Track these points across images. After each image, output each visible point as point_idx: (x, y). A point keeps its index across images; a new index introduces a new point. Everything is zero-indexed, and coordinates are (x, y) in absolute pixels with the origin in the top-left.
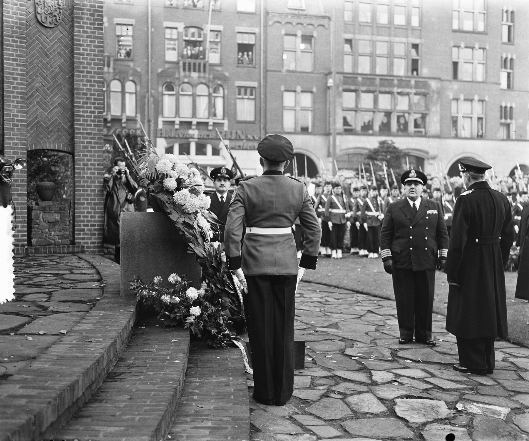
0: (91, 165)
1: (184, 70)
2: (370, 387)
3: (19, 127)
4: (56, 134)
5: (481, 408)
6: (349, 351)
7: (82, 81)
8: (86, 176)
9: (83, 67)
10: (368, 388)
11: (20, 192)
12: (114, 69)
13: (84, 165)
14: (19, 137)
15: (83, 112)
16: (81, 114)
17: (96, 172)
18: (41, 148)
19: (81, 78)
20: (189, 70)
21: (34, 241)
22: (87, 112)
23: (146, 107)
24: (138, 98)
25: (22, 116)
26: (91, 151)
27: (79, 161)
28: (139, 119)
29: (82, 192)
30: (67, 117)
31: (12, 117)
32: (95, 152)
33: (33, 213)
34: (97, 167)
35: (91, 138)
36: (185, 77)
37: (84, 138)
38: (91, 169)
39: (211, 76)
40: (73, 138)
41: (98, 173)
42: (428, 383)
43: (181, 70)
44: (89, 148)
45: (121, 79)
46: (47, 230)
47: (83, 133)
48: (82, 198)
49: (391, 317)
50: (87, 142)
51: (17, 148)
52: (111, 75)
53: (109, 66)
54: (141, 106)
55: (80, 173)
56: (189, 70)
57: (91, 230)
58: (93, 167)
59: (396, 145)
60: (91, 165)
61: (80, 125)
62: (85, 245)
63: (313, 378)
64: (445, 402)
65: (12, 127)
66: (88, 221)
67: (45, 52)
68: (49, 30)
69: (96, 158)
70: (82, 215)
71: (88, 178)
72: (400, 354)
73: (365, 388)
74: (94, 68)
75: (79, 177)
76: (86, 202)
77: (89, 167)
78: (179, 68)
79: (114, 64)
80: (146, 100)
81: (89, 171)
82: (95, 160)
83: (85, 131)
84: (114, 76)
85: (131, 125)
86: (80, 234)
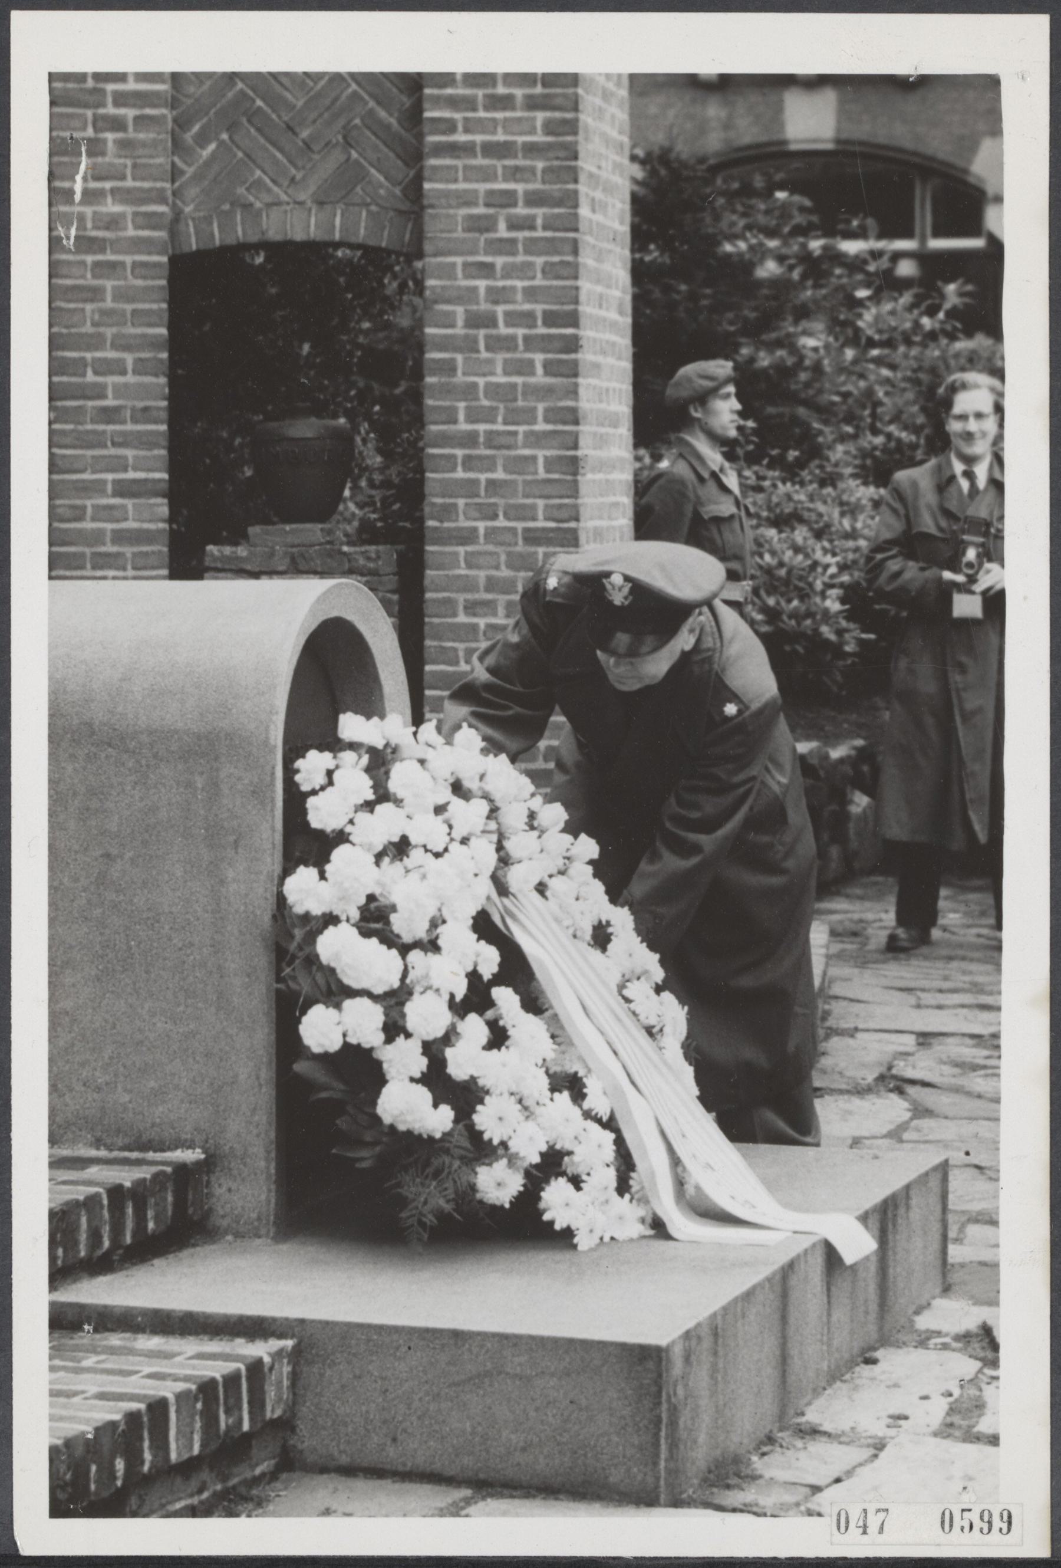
0: (512, 319)
3: (131, 134)
4: (337, 157)
8: (481, 381)
11: (131, 475)
13: (475, 321)
14: (129, 183)
17: (539, 358)
18: (254, 238)
26: (507, 247)
27: (448, 301)
29: (460, 474)
32: (532, 247)
34: (542, 330)
35: (514, 174)
37: (471, 174)
38: (508, 344)
41: (547, 366)
44: (502, 225)
47: (468, 149)
48: (461, 502)
50: (491, 193)
55: (450, 368)
58: (520, 332)
60: (512, 319)
61: (453, 103)
69: (539, 281)
70: (461, 598)
71: (493, 391)
75: (448, 391)
76: (481, 526)
77: (503, 330)
81: (500, 357)
82: (531, 294)
83: (479, 138)
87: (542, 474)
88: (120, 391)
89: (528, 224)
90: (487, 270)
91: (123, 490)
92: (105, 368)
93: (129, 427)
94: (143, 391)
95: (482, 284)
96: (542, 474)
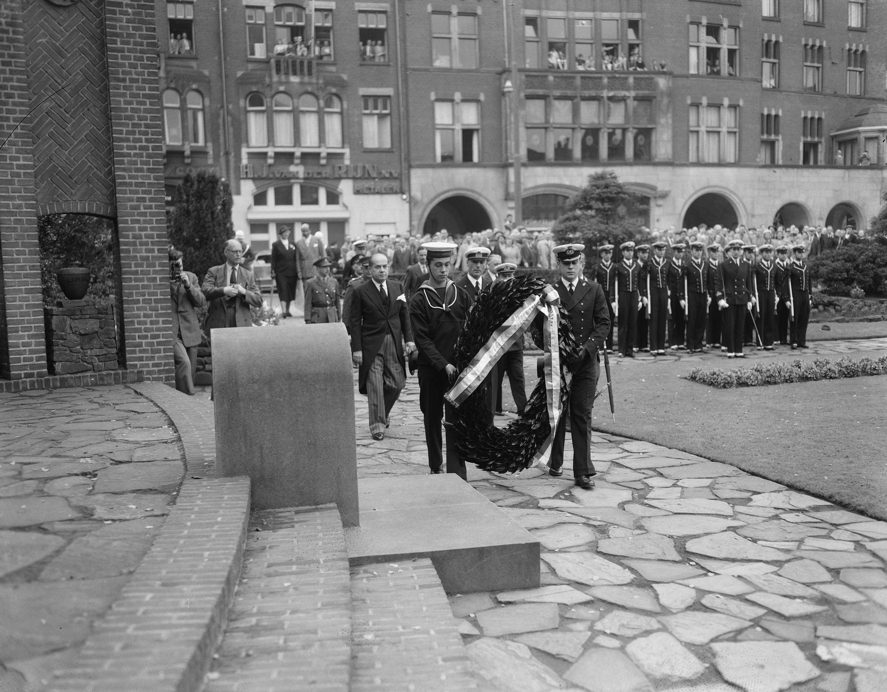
0: (147, 236)
1: (278, 71)
2: (660, 618)
3: (22, 178)
5: (858, 653)
6: (605, 546)
7: (124, 95)
8: (138, 255)
9: (124, 73)
10: (659, 622)
11: (30, 287)
12: (167, 72)
13: (134, 237)
15: (129, 148)
16: (125, 151)
17: (156, 248)
19: (122, 91)
20: (287, 74)
21: (58, 366)
22: (135, 148)
23: (221, 132)
24: (208, 116)
25: (25, 159)
26: (144, 214)
28: (210, 150)
29: (133, 283)
30: (101, 158)
31: (8, 162)
32: (152, 214)
33: (55, 320)
35: (144, 192)
36: (280, 83)
37: (131, 192)
38: (146, 244)
39: (321, 81)
40: (113, 193)
41: (158, 250)
42: (754, 603)
43: (274, 71)
44: (142, 208)
45: (179, 89)
46: (79, 347)
47: (130, 184)
49: (651, 473)
50: (138, 198)
51: (21, 214)
54: (212, 132)
56: (287, 74)
57: (152, 344)
59: (620, 181)
61: (124, 170)
62: (145, 369)
63: (563, 606)
64: (797, 643)
65: (9, 177)
66: (146, 330)
67: (58, 48)
68: (61, 11)
71: (142, 258)
72: (691, 546)
73: (653, 623)
74: (142, 74)
75: (128, 258)
76: (141, 298)
77: (144, 240)
78: (270, 70)
79: (166, 65)
80: (221, 121)
82: (152, 229)
83: (134, 181)
84: (167, 83)
85: (199, 161)
86: (134, 352)
87: (158, 282)
88: (25, 260)
89: (150, 207)
90: (138, 221)
91: (28, 291)
92: (19, 253)
93: (29, 272)
94: (32, 261)
95: (137, 226)
96: (158, 282)
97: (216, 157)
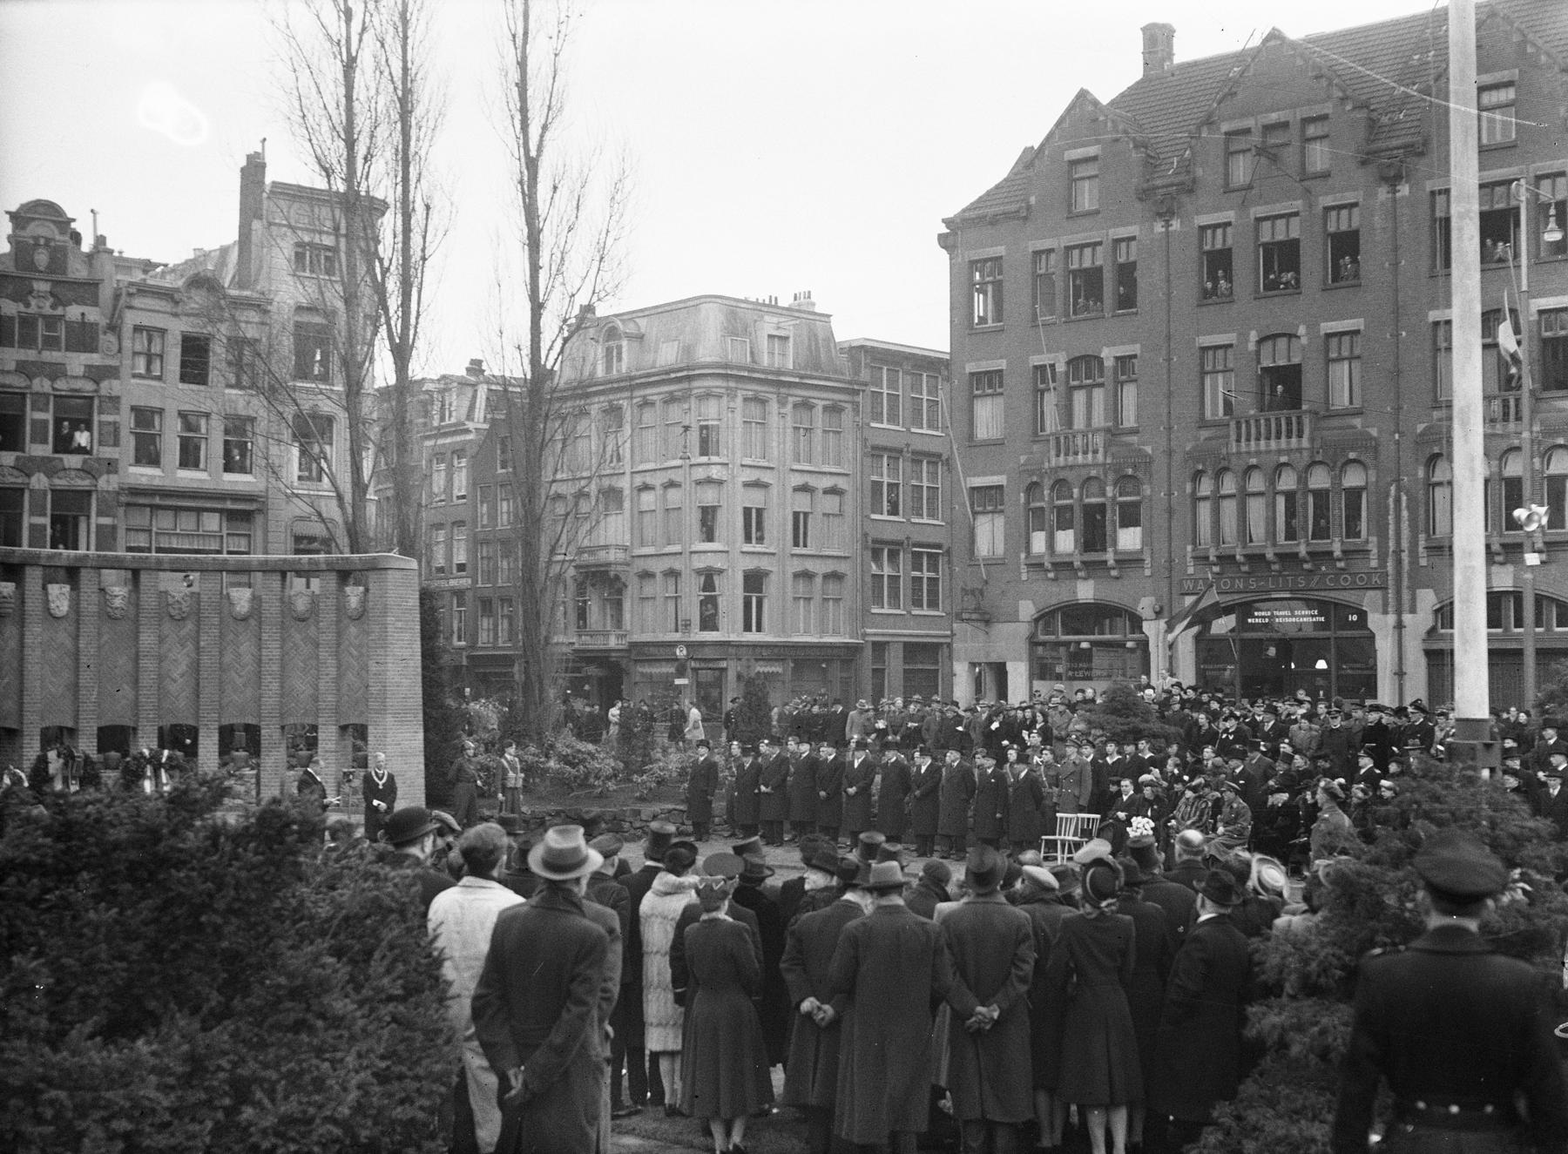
12: (1312, 440)
23: (1391, 518)
52: (1305, 454)
53: (1300, 436)
80: (1391, 500)
85: (1358, 566)
97: (1383, 558)
